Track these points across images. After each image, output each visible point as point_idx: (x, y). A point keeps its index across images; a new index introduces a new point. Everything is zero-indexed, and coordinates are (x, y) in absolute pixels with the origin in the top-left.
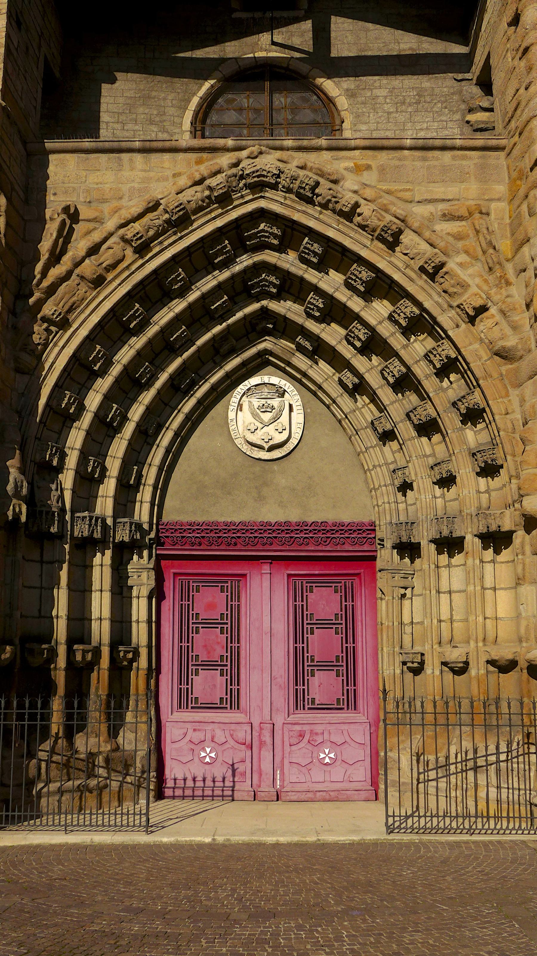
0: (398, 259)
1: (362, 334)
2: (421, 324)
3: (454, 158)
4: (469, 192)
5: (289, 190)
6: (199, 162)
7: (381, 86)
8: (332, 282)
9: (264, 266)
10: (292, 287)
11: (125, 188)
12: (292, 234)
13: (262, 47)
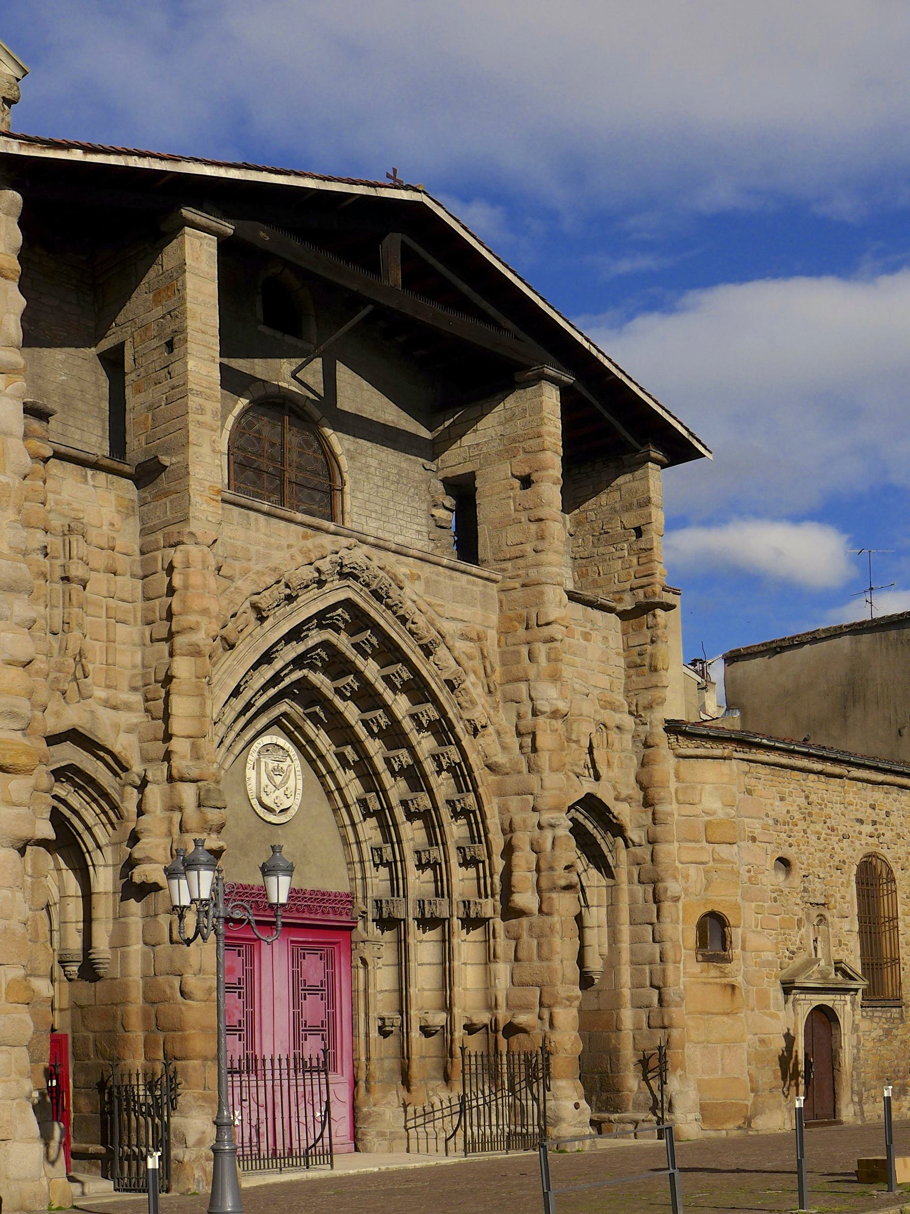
3: (468, 582)
5: (367, 585)
6: (305, 537)
11: (253, 549)
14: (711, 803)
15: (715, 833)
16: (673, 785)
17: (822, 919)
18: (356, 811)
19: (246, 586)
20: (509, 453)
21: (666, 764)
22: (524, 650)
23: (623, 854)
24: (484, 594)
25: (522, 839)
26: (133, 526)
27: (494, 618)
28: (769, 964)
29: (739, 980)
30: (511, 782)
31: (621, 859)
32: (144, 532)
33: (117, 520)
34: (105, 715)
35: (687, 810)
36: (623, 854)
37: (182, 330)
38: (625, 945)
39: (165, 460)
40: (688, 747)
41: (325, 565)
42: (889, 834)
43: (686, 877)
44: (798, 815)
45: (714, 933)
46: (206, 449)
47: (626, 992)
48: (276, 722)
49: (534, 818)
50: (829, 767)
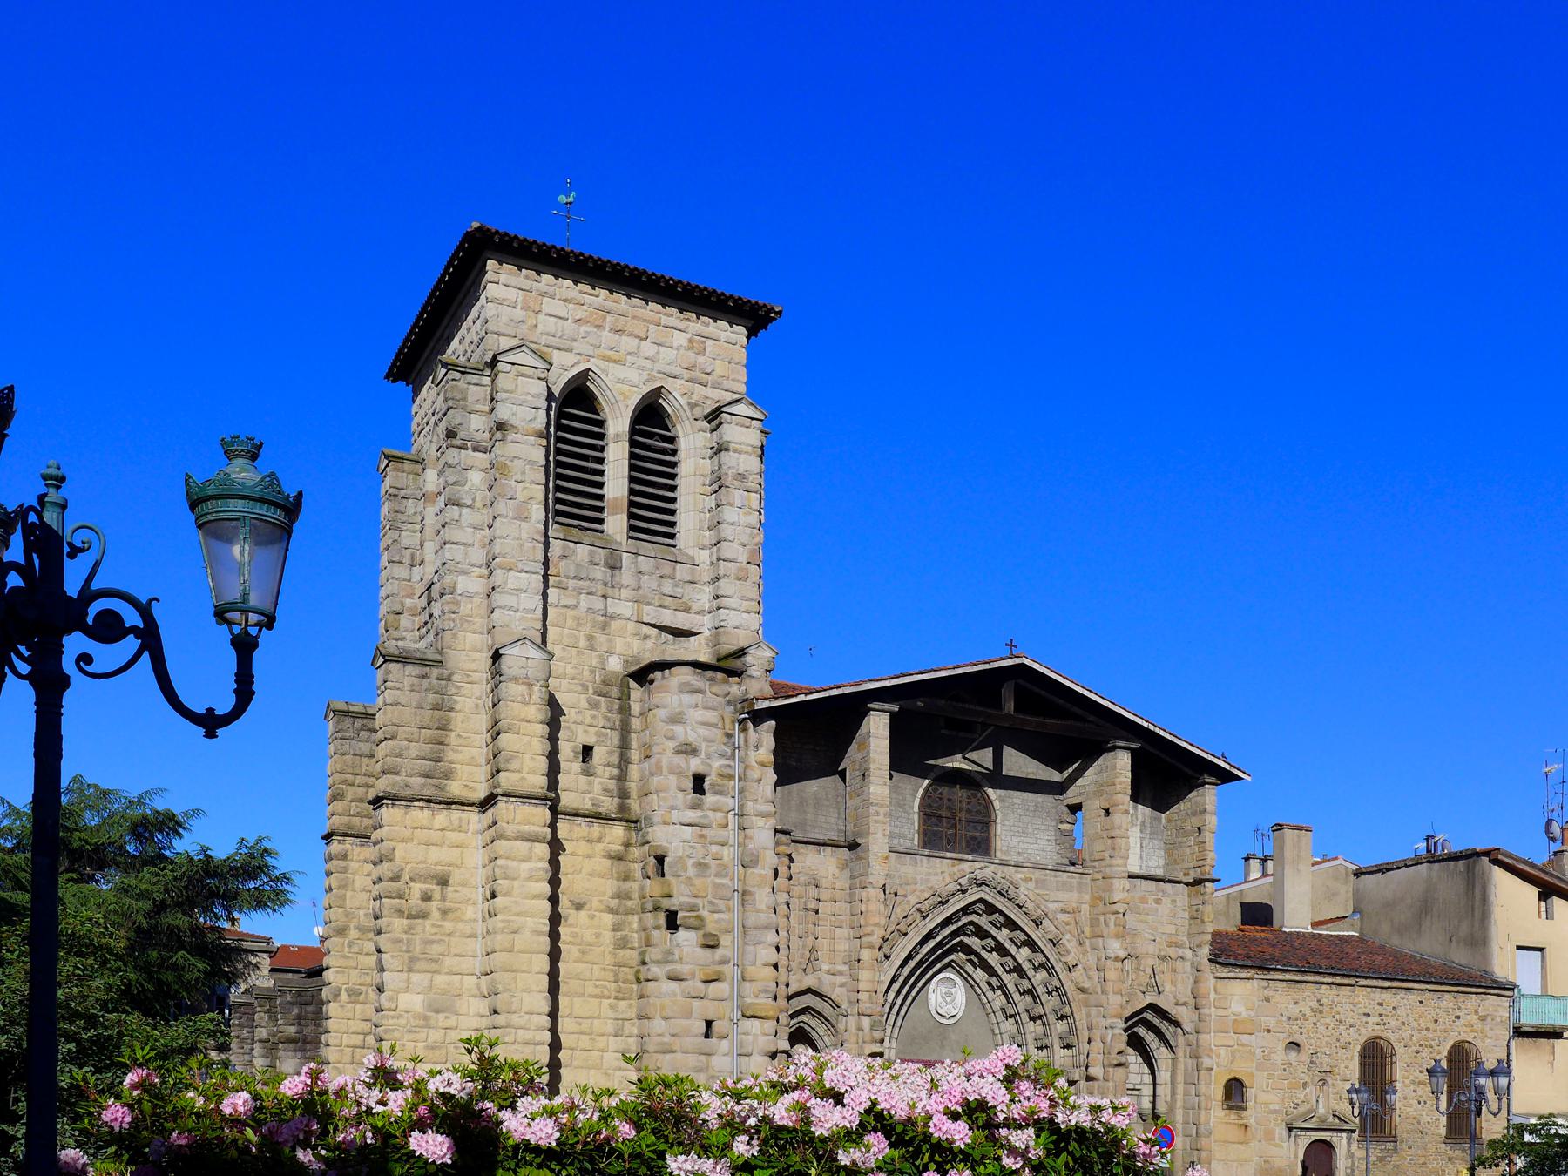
0: (1039, 932)
1: (1012, 964)
2: (1046, 966)
4: (1071, 897)
7: (1018, 797)
8: (1003, 935)
9: (971, 923)
10: (982, 933)
12: (991, 909)
13: (957, 762)
15: (1238, 1027)
16: (1212, 996)
17: (1324, 1082)
18: (1000, 1015)
19: (913, 900)
21: (1209, 983)
22: (1102, 918)
23: (1181, 1039)
24: (1080, 883)
25: (1097, 1035)
26: (847, 873)
28: (1276, 1111)
29: (1251, 1122)
30: (1092, 998)
31: (1180, 1041)
32: (852, 877)
33: (837, 872)
35: (1222, 1012)
36: (1181, 1039)
37: (867, 769)
38: (1180, 1096)
39: (859, 840)
40: (1224, 972)
41: (964, 881)
42: (1394, 1023)
43: (1218, 1056)
44: (1308, 1013)
45: (1235, 1091)
46: (880, 835)
47: (1179, 1126)
48: (948, 965)
49: (1103, 1022)
50: (1338, 980)
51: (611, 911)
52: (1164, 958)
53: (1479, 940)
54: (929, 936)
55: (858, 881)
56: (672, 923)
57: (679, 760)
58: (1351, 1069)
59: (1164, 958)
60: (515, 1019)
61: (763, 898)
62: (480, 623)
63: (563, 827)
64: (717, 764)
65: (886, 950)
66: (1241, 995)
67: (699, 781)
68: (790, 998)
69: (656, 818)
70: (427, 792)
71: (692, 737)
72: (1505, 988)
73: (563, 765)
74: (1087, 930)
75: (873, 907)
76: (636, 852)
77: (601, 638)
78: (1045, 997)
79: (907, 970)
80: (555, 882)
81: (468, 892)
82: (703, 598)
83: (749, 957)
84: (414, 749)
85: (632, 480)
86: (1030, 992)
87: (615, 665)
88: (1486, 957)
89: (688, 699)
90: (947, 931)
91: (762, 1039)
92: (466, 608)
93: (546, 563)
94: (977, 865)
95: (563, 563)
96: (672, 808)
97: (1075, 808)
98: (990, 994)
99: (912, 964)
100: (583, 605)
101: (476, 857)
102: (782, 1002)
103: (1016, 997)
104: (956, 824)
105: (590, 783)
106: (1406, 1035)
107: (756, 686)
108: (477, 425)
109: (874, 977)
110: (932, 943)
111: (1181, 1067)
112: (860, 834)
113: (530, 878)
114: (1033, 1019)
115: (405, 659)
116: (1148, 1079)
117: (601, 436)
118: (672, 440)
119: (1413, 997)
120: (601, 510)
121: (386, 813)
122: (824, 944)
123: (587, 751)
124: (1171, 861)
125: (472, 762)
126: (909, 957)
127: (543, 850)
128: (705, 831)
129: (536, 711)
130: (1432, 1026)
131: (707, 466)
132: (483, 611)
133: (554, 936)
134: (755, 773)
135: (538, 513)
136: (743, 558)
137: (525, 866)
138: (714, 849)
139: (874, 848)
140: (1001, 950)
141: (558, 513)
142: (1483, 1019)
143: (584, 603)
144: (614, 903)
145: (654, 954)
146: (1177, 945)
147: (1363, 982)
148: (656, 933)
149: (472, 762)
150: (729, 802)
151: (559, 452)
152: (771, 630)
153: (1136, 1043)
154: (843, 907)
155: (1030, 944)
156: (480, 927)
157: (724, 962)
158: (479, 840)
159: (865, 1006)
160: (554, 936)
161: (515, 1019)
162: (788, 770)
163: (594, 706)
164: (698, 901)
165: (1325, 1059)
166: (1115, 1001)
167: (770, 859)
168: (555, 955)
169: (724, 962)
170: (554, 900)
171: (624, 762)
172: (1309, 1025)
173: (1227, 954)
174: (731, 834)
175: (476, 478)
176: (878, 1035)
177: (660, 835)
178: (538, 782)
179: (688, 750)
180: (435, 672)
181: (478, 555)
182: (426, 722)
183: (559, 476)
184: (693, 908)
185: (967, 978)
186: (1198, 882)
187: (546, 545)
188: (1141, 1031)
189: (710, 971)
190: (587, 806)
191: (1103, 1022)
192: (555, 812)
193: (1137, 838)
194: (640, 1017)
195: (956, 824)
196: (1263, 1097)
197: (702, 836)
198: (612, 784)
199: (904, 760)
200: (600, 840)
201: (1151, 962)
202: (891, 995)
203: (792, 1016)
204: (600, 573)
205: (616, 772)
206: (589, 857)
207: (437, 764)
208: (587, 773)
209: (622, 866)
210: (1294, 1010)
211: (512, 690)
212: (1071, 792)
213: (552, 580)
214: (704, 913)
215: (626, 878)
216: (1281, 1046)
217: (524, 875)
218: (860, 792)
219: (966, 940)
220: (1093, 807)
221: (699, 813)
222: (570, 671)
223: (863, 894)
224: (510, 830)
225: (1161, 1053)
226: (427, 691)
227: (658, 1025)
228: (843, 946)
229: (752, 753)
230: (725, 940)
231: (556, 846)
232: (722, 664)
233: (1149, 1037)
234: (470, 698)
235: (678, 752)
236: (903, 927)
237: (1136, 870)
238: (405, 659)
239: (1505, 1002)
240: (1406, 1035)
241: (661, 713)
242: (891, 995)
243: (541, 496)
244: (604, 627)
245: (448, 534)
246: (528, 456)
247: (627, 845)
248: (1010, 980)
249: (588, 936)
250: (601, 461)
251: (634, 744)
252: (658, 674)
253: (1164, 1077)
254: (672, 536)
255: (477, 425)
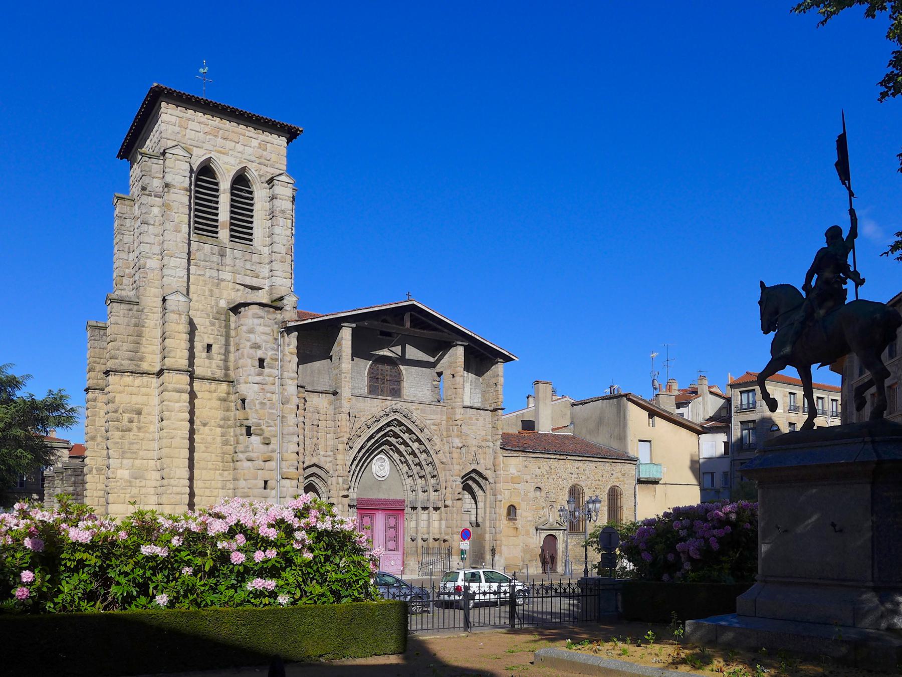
0: (423, 435)
1: (411, 451)
2: (426, 451)
4: (437, 417)
7: (414, 369)
8: (406, 436)
9: (391, 430)
10: (396, 436)
12: (400, 424)
13: (385, 352)
14: (513, 470)
15: (514, 480)
16: (502, 465)
19: (363, 419)
20: (450, 367)
23: (488, 486)
26: (332, 407)
27: (445, 417)
31: (487, 487)
34: (323, 459)
35: (506, 473)
36: (488, 486)
40: (506, 453)
41: (387, 410)
44: (545, 473)
45: (512, 510)
49: (452, 478)
50: (558, 457)
51: (220, 427)
52: (480, 447)
53: (622, 437)
54: (371, 437)
55: (337, 411)
56: (249, 433)
57: (252, 351)
58: (563, 498)
59: (480, 447)
60: (172, 482)
61: (291, 419)
62: (157, 283)
63: (197, 385)
64: (270, 353)
65: (351, 444)
66: (514, 464)
67: (261, 362)
68: (304, 469)
69: (241, 381)
70: (131, 368)
71: (258, 340)
72: (633, 460)
73: (197, 354)
74: (445, 434)
75: (344, 423)
76: (233, 397)
77: (216, 291)
78: (425, 467)
79: (361, 454)
80: (192, 413)
81: (151, 418)
82: (265, 271)
83: (285, 449)
84: (125, 346)
85: (232, 212)
86: (419, 464)
87: (223, 304)
88: (625, 446)
89: (256, 321)
90: (380, 435)
91: (291, 489)
92: (151, 276)
93: (189, 254)
94: (394, 402)
95: (198, 253)
96: (249, 375)
97: (440, 374)
98: (401, 465)
99: (363, 451)
100: (208, 274)
101: (156, 400)
102: (301, 471)
103: (413, 466)
104: (385, 383)
105: (210, 363)
106: (589, 483)
107: (290, 315)
108: (156, 184)
109: (345, 458)
110: (373, 441)
111: (488, 500)
112: (337, 387)
113: (180, 411)
114: (421, 477)
115: (121, 301)
116: (474, 506)
117: (217, 190)
118: (251, 193)
119: (592, 465)
120: (217, 227)
121: (111, 378)
122: (321, 441)
123: (209, 347)
124: (484, 400)
125: (153, 353)
126: (362, 448)
127: (186, 397)
128: (264, 386)
129: (183, 327)
130: (601, 479)
131: (267, 206)
132: (159, 277)
133: (191, 440)
134: (288, 358)
135: (185, 228)
136: (284, 252)
137: (177, 405)
138: (269, 395)
139: (344, 394)
140: (407, 445)
141: (196, 228)
142: (624, 475)
143: (208, 273)
144: (222, 423)
145: (240, 448)
146: (486, 440)
147: (569, 458)
148: (241, 437)
149: (153, 353)
150: (276, 372)
151: (197, 198)
152: (298, 289)
153: (467, 488)
154: (330, 423)
155: (418, 440)
156: (157, 436)
157: (273, 451)
158: (157, 392)
159: (340, 472)
160: (191, 440)
161: (172, 482)
162: (304, 357)
163: (213, 324)
164: (261, 421)
165: (553, 495)
166: (457, 467)
167: (295, 400)
168: (192, 450)
169: (273, 451)
170: (192, 422)
171: (227, 352)
172: (545, 479)
173: (510, 444)
174: (276, 388)
175: (156, 211)
176: (346, 486)
177: (243, 389)
178: (184, 363)
179: (256, 346)
180: (136, 307)
181: (157, 249)
182: (131, 333)
183: (196, 210)
184: (258, 425)
185: (390, 457)
186: (495, 410)
187: (189, 245)
188: (470, 482)
189: (266, 456)
190: (209, 374)
191: (452, 478)
192: (192, 377)
193: (468, 389)
194: (234, 479)
195: (385, 383)
196: (525, 514)
197: (263, 389)
198: (221, 363)
199: (358, 352)
200: (215, 391)
201: (474, 449)
202: (354, 466)
203: (306, 478)
204: (216, 258)
205: (223, 357)
206: (210, 400)
207: (136, 354)
208: (209, 358)
209: (225, 404)
210: (538, 472)
211: (171, 317)
212: (438, 367)
213: (192, 262)
214: (264, 427)
215: (228, 410)
216: (533, 489)
217: (177, 409)
218: (338, 367)
219: (389, 439)
220: (447, 374)
221: (262, 378)
222: (201, 307)
223: (339, 417)
224: (170, 387)
225: (479, 493)
226: (131, 317)
227: (242, 483)
228: (331, 443)
229: (286, 348)
230: (273, 441)
231: (193, 395)
232: (274, 304)
233: (474, 486)
234: (152, 320)
235: (252, 348)
236: (359, 433)
237: (467, 404)
238: (121, 301)
239: (634, 467)
240: (589, 483)
241: (244, 328)
242: (354, 466)
243: (187, 220)
244: (218, 285)
245: (142, 238)
246: (180, 200)
247: (228, 394)
248: (410, 458)
249: (209, 439)
250: (217, 203)
251: (232, 343)
252: (243, 309)
253: (480, 505)
254: (251, 240)
255: (156, 184)
